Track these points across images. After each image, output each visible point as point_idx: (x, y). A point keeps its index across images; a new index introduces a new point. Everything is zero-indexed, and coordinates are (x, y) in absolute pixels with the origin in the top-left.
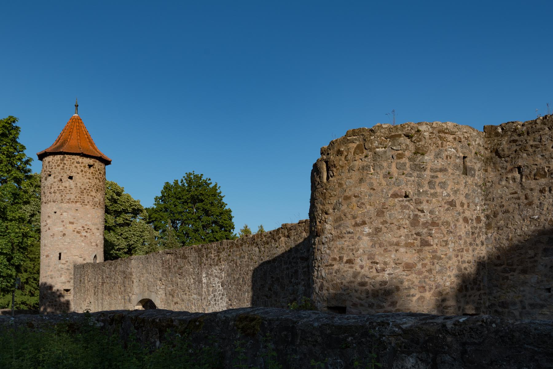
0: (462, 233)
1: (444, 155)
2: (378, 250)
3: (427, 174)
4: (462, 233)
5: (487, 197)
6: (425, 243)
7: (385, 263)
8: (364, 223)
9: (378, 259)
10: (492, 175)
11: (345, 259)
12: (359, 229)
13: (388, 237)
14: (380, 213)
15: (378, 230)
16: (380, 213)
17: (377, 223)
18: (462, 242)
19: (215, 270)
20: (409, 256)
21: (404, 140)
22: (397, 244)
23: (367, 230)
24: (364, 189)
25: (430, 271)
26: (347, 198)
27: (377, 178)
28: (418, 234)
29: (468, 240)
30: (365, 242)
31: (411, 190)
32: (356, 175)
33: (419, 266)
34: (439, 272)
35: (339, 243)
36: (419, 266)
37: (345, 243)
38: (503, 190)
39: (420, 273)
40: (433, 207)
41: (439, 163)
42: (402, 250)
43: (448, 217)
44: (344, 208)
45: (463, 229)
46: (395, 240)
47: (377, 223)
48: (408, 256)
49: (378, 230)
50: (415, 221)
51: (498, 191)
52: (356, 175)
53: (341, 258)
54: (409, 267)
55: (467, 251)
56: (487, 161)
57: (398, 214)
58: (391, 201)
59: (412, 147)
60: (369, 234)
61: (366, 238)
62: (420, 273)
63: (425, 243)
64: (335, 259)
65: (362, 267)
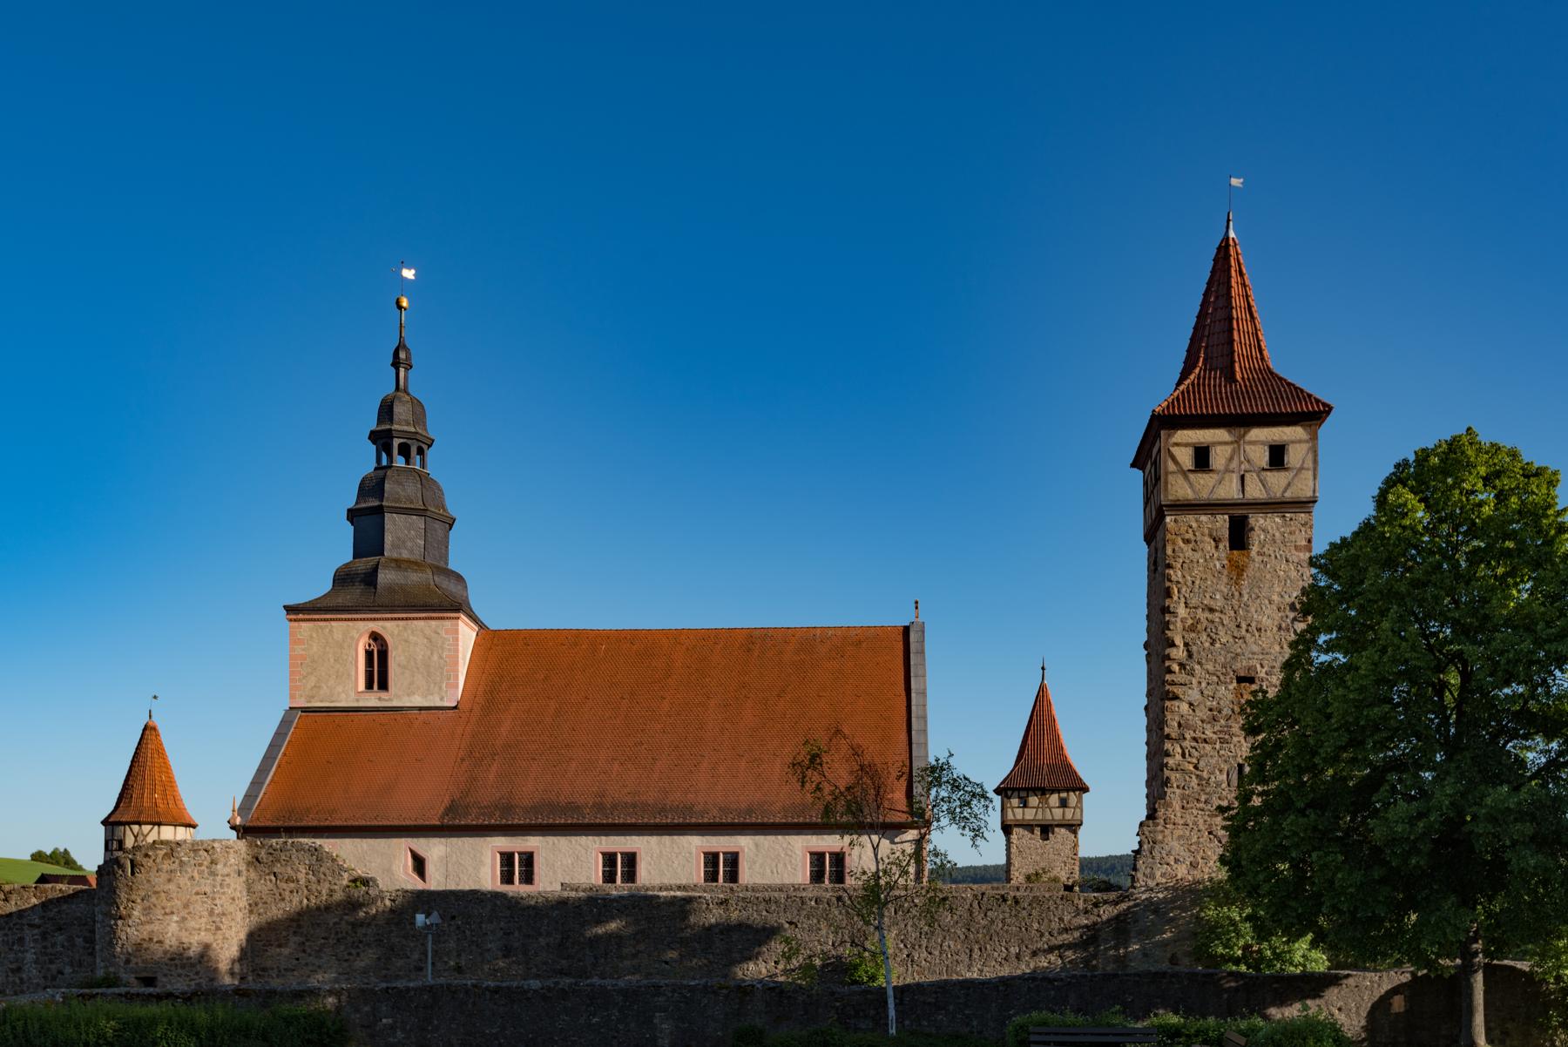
3: (219, 878)
5: (249, 891)
6: (218, 928)
10: (253, 875)
13: (192, 924)
14: (186, 906)
16: (186, 906)
17: (184, 913)
23: (175, 918)
24: (172, 887)
26: (156, 893)
27: (183, 881)
30: (173, 928)
31: (208, 890)
32: (164, 876)
35: (148, 927)
37: (155, 927)
38: (264, 886)
40: (223, 903)
41: (226, 870)
43: (231, 909)
44: (153, 899)
45: (239, 916)
47: (184, 913)
48: (205, 937)
49: (184, 919)
50: (211, 913)
51: (258, 887)
52: (164, 876)
54: (207, 947)
56: (249, 864)
57: (200, 907)
58: (195, 898)
63: (218, 928)
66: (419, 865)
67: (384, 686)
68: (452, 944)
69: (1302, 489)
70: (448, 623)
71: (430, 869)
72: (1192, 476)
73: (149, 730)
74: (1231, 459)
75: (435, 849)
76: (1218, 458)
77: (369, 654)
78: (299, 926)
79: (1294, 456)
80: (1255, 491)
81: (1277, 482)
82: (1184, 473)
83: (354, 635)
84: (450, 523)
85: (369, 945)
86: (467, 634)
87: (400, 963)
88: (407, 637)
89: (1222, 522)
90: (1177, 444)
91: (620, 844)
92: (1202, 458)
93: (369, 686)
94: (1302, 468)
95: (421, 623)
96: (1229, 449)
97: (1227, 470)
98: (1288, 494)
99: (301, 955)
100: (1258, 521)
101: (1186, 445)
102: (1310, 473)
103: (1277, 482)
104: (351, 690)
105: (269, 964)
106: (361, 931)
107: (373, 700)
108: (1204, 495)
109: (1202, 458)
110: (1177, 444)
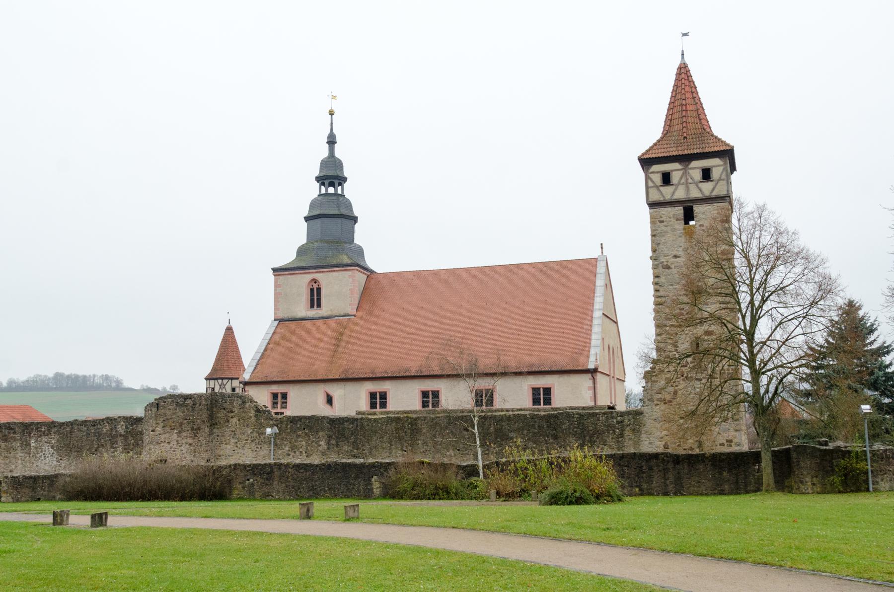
15: (180, 432)
19: (44, 439)
20: (190, 441)
50: (192, 429)
66: (330, 400)
67: (319, 306)
69: (720, 191)
70: (350, 273)
71: (335, 401)
72: (662, 189)
73: (229, 330)
74: (681, 178)
75: (337, 391)
76: (675, 178)
77: (312, 290)
79: (716, 174)
80: (695, 194)
81: (707, 188)
82: (657, 187)
83: (302, 281)
84: (355, 219)
86: (361, 277)
87: (280, 452)
88: (330, 281)
89: (679, 211)
90: (653, 172)
91: (430, 385)
92: (666, 179)
93: (312, 306)
94: (720, 180)
95: (336, 274)
96: (681, 172)
97: (679, 184)
98: (714, 194)
100: (698, 209)
101: (657, 172)
102: (724, 182)
103: (707, 188)
104: (302, 309)
105: (221, 453)
107: (313, 313)
108: (668, 197)
109: (666, 179)
110: (653, 172)
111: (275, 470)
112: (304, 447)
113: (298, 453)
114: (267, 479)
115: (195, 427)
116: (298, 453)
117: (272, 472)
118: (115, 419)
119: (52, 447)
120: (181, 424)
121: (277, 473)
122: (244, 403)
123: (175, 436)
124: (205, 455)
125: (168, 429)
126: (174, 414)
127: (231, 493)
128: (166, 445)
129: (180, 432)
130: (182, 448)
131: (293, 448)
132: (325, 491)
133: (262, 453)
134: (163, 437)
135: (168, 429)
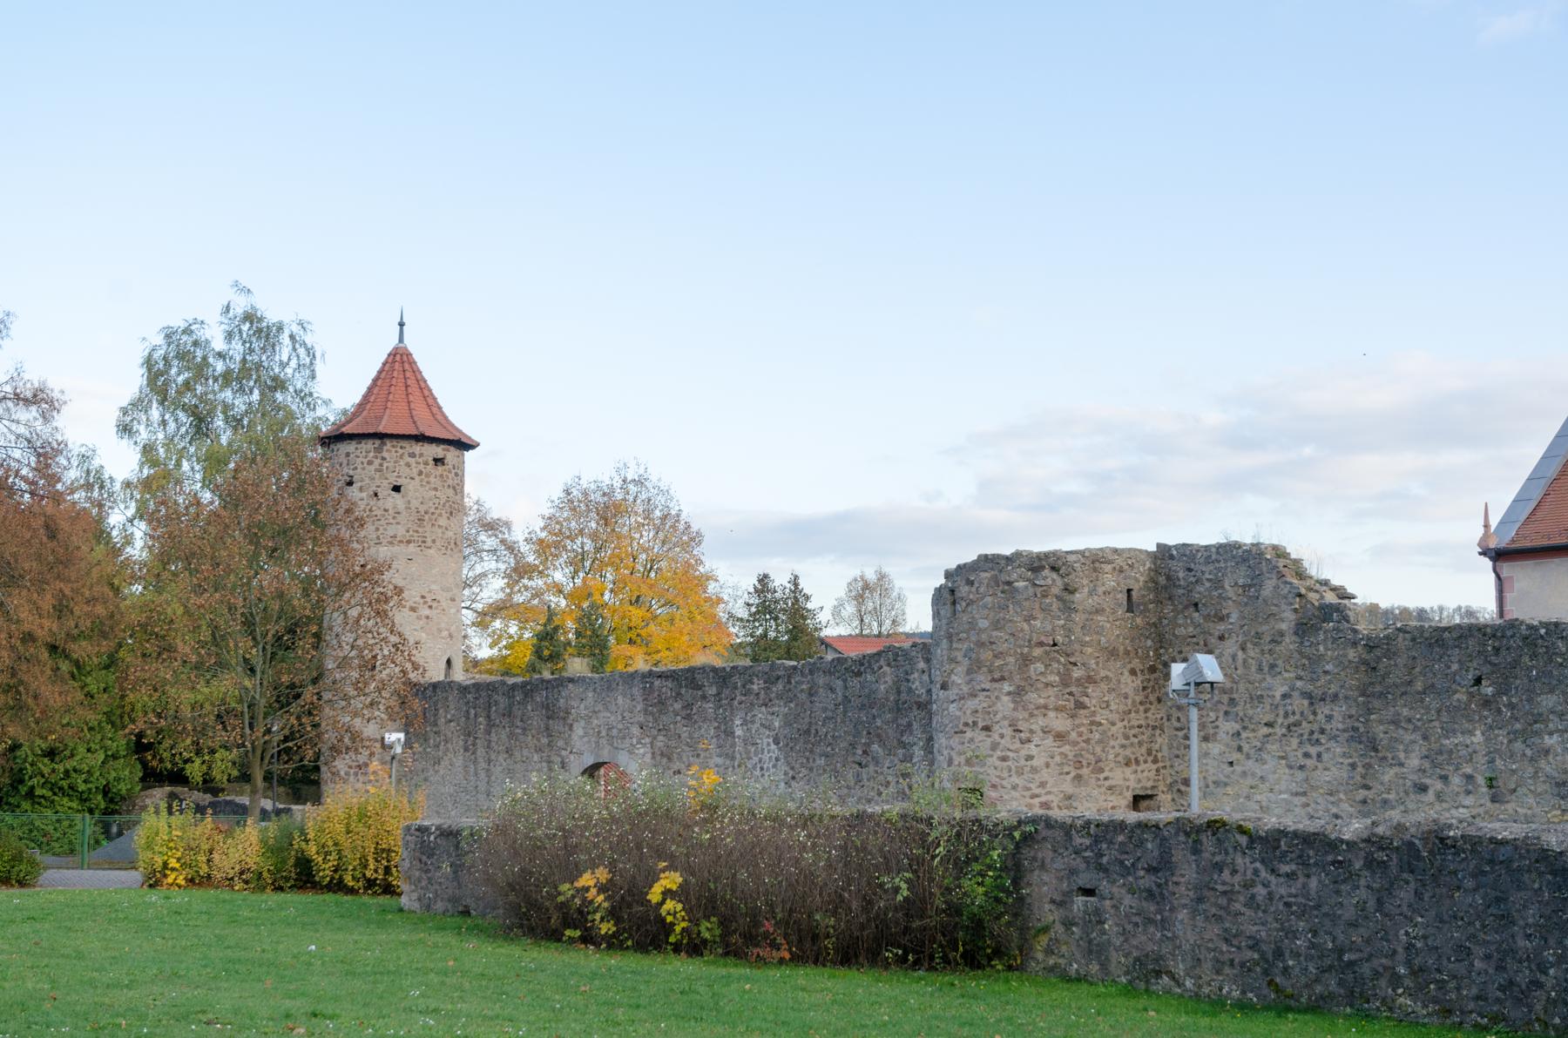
0: (1129, 690)
1: (1101, 590)
2: (1021, 715)
4: (1129, 690)
6: (1080, 706)
7: (1031, 731)
8: (1002, 679)
9: (1022, 725)
11: (980, 725)
12: (996, 685)
18: (1129, 702)
19: (761, 714)
20: (1060, 723)
21: (1046, 572)
22: (1046, 707)
23: (1007, 687)
25: (1087, 741)
28: (1070, 694)
29: (1138, 699)
33: (1074, 735)
34: (1100, 742)
36: (1074, 735)
39: (1075, 743)
42: (1052, 714)
46: (1042, 701)
53: (975, 723)
55: (1137, 712)
59: (1059, 582)
60: (1009, 693)
61: (1006, 699)
62: (1075, 743)
63: (1080, 706)
64: (966, 724)
65: (1002, 736)
68: (1478, 737)
78: (1232, 701)
85: (1335, 738)
87: (1389, 774)
99: (1235, 756)
106: (1323, 710)
111: (1178, 855)
112: (1481, 759)
113: (1456, 780)
114: (1150, 895)
115: (1077, 673)
116: (1456, 780)
117: (1162, 866)
118: (906, 653)
119: (776, 742)
120: (1026, 661)
121: (1187, 873)
122: (1255, 582)
123: (1005, 705)
124: (1132, 780)
125: (982, 679)
126: (997, 625)
127: (1025, 949)
128: (980, 736)
129: (1018, 693)
130: (1032, 749)
131: (1437, 759)
132: (1396, 980)
133: (1324, 777)
134: (971, 704)
135: (982, 679)
